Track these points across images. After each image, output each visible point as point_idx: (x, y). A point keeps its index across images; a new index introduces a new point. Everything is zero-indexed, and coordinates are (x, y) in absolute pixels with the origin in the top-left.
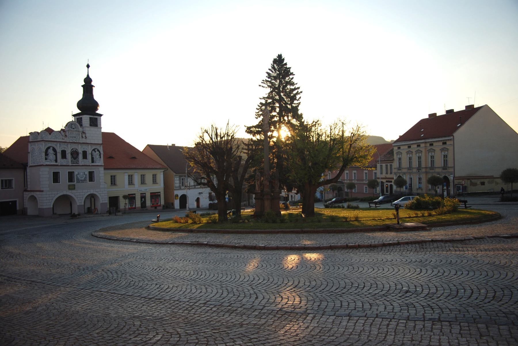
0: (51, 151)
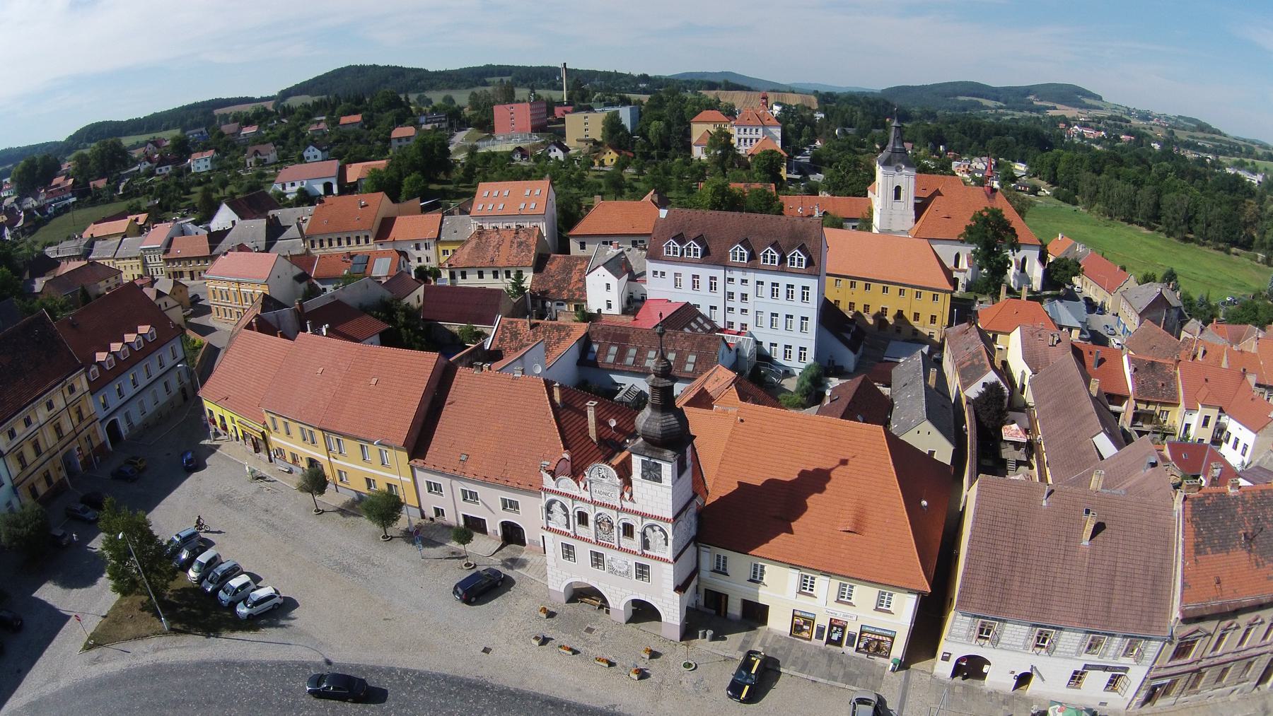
0: (556, 508)
